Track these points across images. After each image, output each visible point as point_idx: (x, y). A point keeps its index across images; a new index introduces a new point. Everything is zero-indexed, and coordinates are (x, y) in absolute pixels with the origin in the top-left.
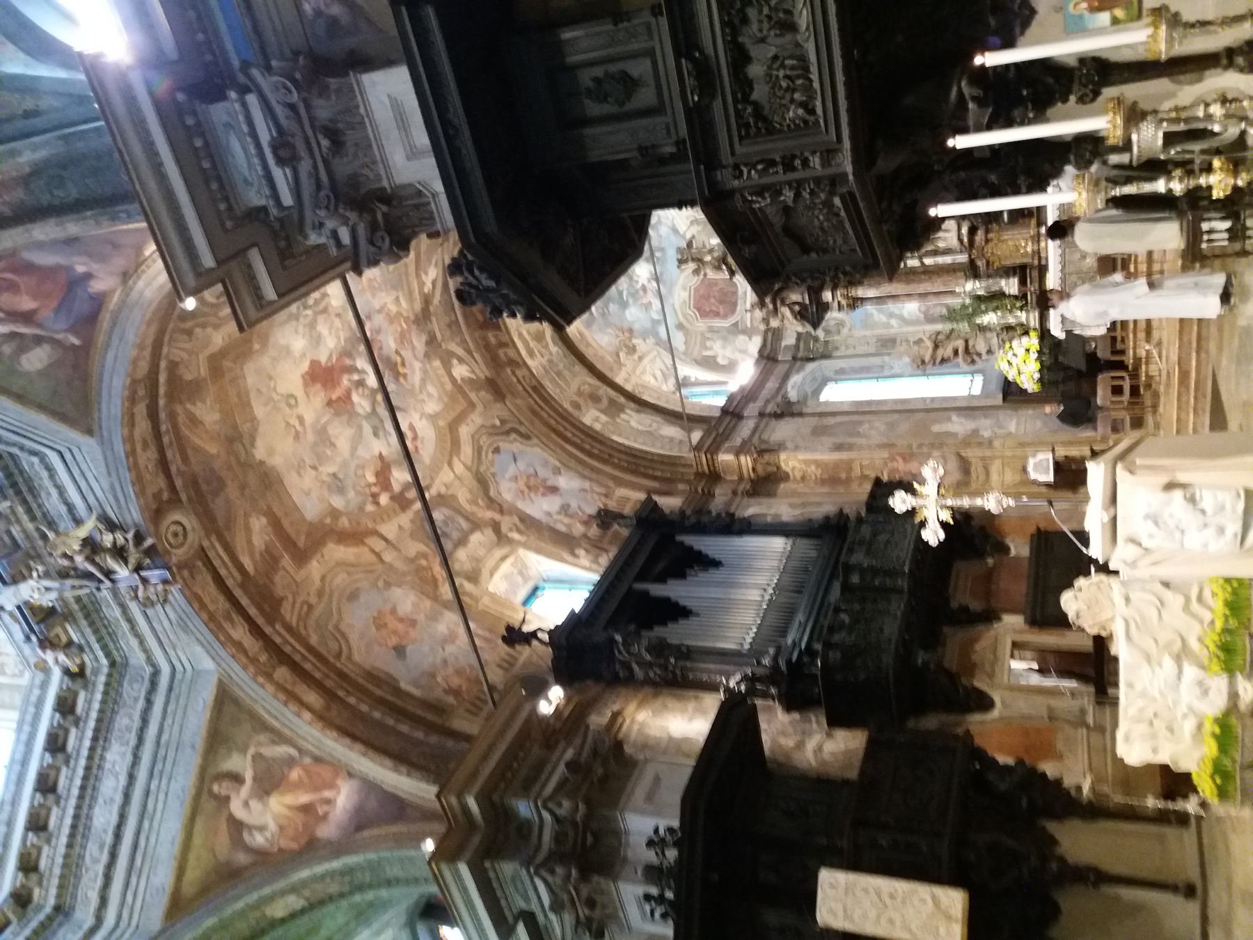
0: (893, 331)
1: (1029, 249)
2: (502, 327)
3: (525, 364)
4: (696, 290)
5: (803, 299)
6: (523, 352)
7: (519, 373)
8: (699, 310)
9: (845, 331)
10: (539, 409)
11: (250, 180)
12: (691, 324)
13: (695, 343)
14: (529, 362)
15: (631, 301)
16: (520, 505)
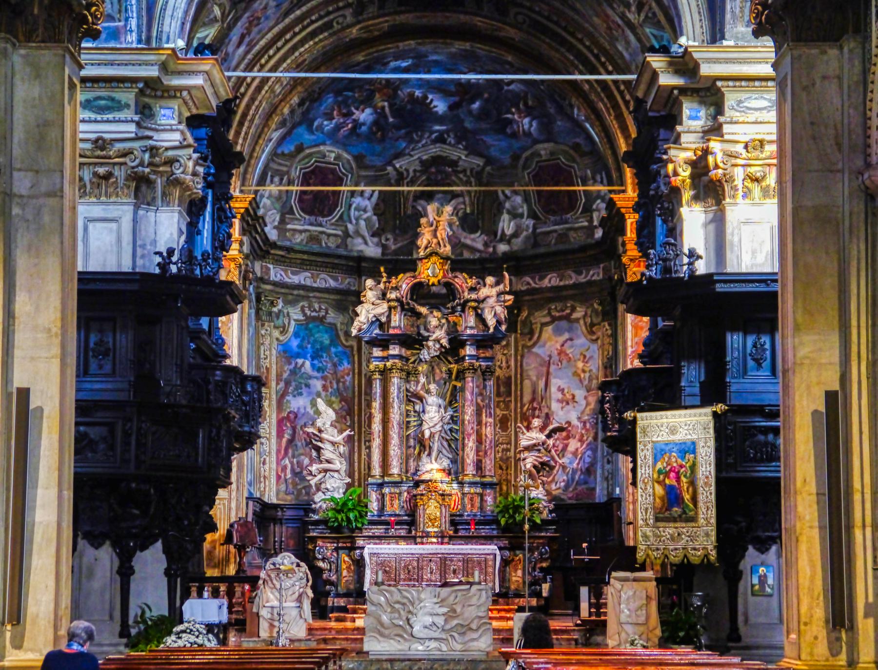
0: (273, 384)
1: (429, 530)
2: (403, 8)
3: (359, 22)
4: (333, 171)
5: (394, 328)
6: (370, 22)
7: (348, 12)
8: (313, 172)
9: (276, 333)
10: (305, 23)
11: (741, 105)
12: (299, 161)
13: (280, 164)
14: (358, 27)
15: (340, 99)
16: (246, 15)
